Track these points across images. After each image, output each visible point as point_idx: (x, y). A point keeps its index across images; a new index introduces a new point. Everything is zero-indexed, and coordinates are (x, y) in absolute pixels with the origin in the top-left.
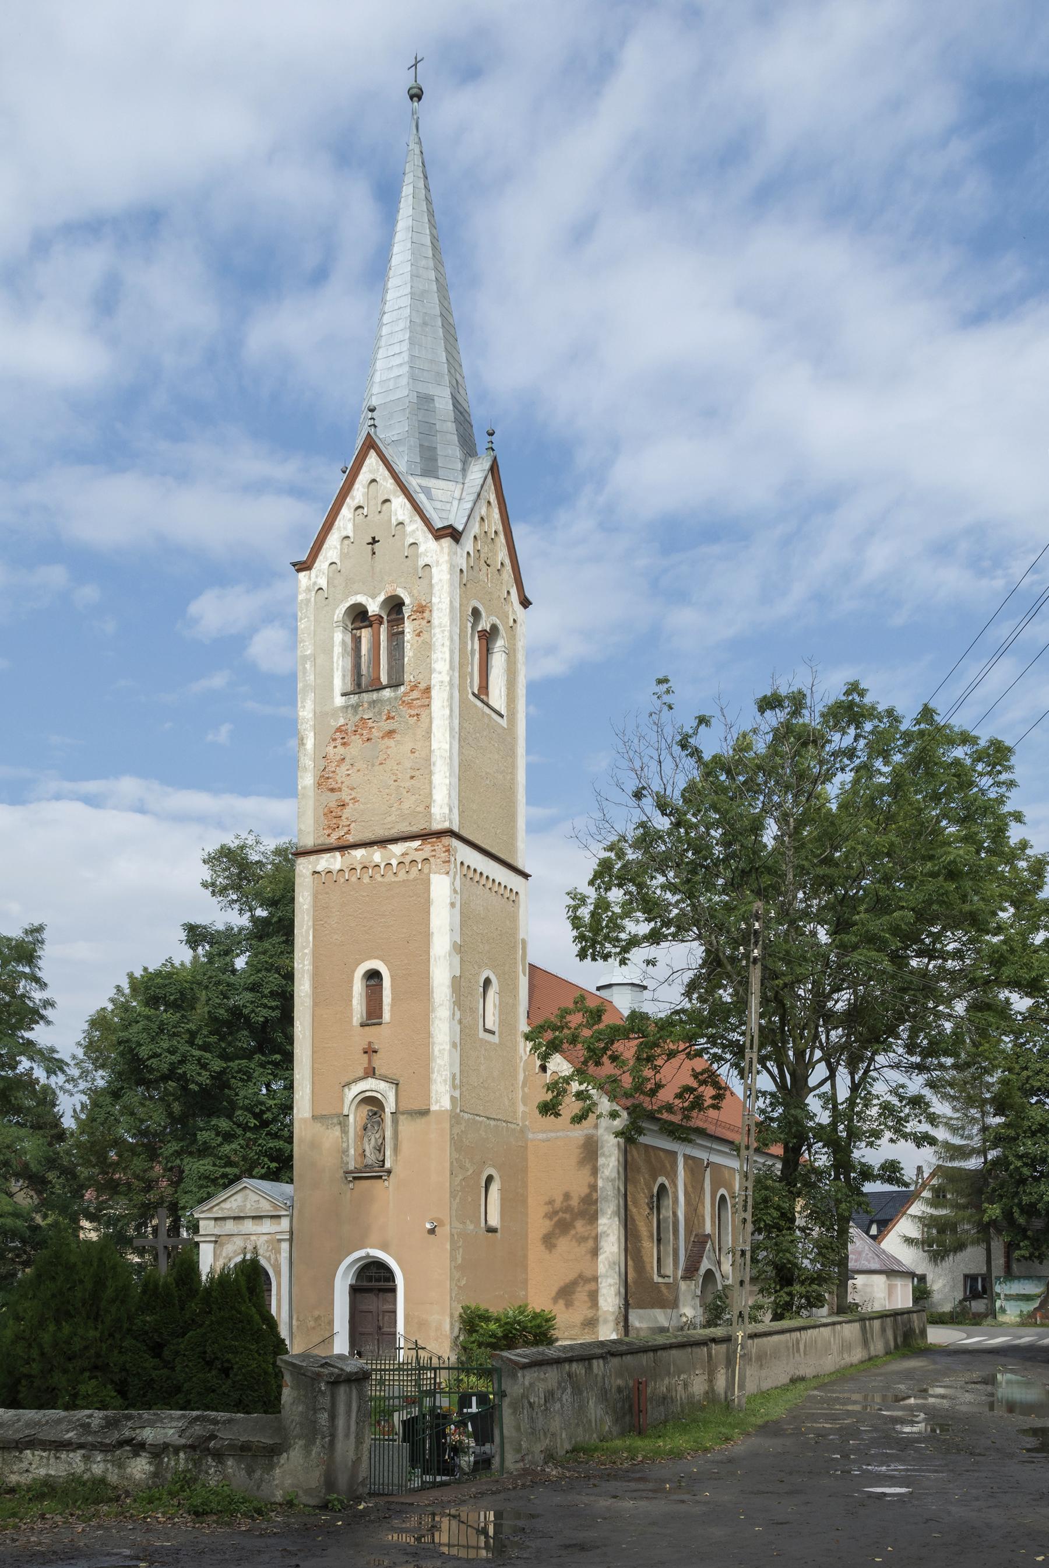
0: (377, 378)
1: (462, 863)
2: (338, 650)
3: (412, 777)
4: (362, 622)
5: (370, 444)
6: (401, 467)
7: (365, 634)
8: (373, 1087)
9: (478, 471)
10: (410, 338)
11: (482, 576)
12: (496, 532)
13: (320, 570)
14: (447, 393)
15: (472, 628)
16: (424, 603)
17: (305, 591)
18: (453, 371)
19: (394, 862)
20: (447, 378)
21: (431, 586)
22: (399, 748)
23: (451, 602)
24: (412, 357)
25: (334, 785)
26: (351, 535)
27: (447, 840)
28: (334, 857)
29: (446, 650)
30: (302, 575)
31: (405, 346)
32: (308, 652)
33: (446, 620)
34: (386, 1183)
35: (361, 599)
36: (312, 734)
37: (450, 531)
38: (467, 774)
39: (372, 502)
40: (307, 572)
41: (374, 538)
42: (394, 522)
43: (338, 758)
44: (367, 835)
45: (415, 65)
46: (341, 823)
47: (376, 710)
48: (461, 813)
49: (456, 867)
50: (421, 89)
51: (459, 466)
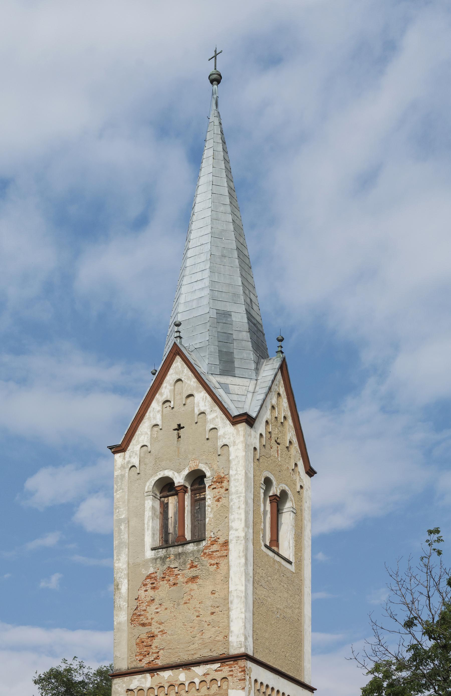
0: (182, 300)
1: (256, 681)
2: (148, 514)
3: (212, 613)
4: (169, 491)
5: (176, 351)
6: (203, 368)
7: (172, 501)
9: (269, 369)
10: (210, 268)
11: (273, 452)
12: (285, 418)
13: (133, 452)
14: (242, 309)
15: (265, 493)
17: (120, 469)
18: (247, 292)
19: (197, 681)
20: (242, 297)
21: (229, 461)
22: (202, 590)
23: (246, 474)
24: (213, 282)
25: (145, 621)
26: (159, 423)
27: (242, 663)
28: (145, 678)
29: (242, 512)
30: (117, 456)
31: (206, 274)
32: (123, 517)
33: (242, 488)
35: (168, 473)
36: (126, 581)
37: (245, 417)
38: (260, 609)
39: (178, 397)
40: (123, 453)
41: (179, 425)
42: (197, 412)
43: (148, 599)
44: (174, 659)
45: (215, 57)
46: (151, 651)
47: (182, 560)
48: (255, 641)
49: (250, 683)
50: (220, 75)
51: (253, 366)
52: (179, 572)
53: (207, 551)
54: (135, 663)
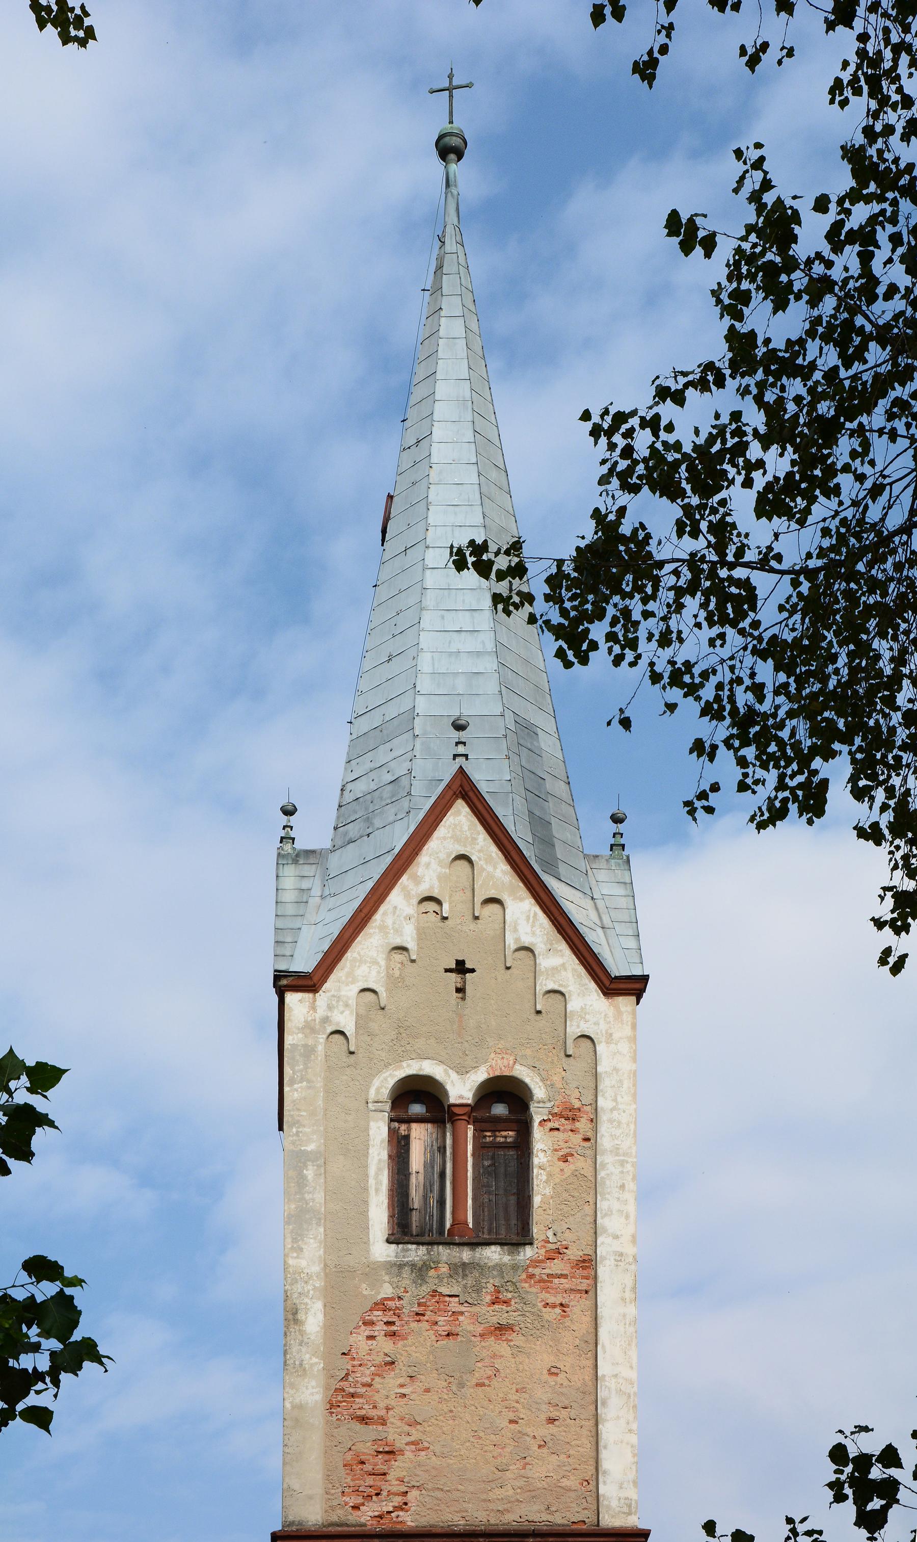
3: (551, 1421)
16: (577, 1104)
25: (367, 1411)
36: (318, 1306)
43: (379, 1359)
44: (449, 1517)
46: (386, 1488)
47: (470, 1281)
52: (462, 1309)
53: (537, 1271)
54: (340, 1512)
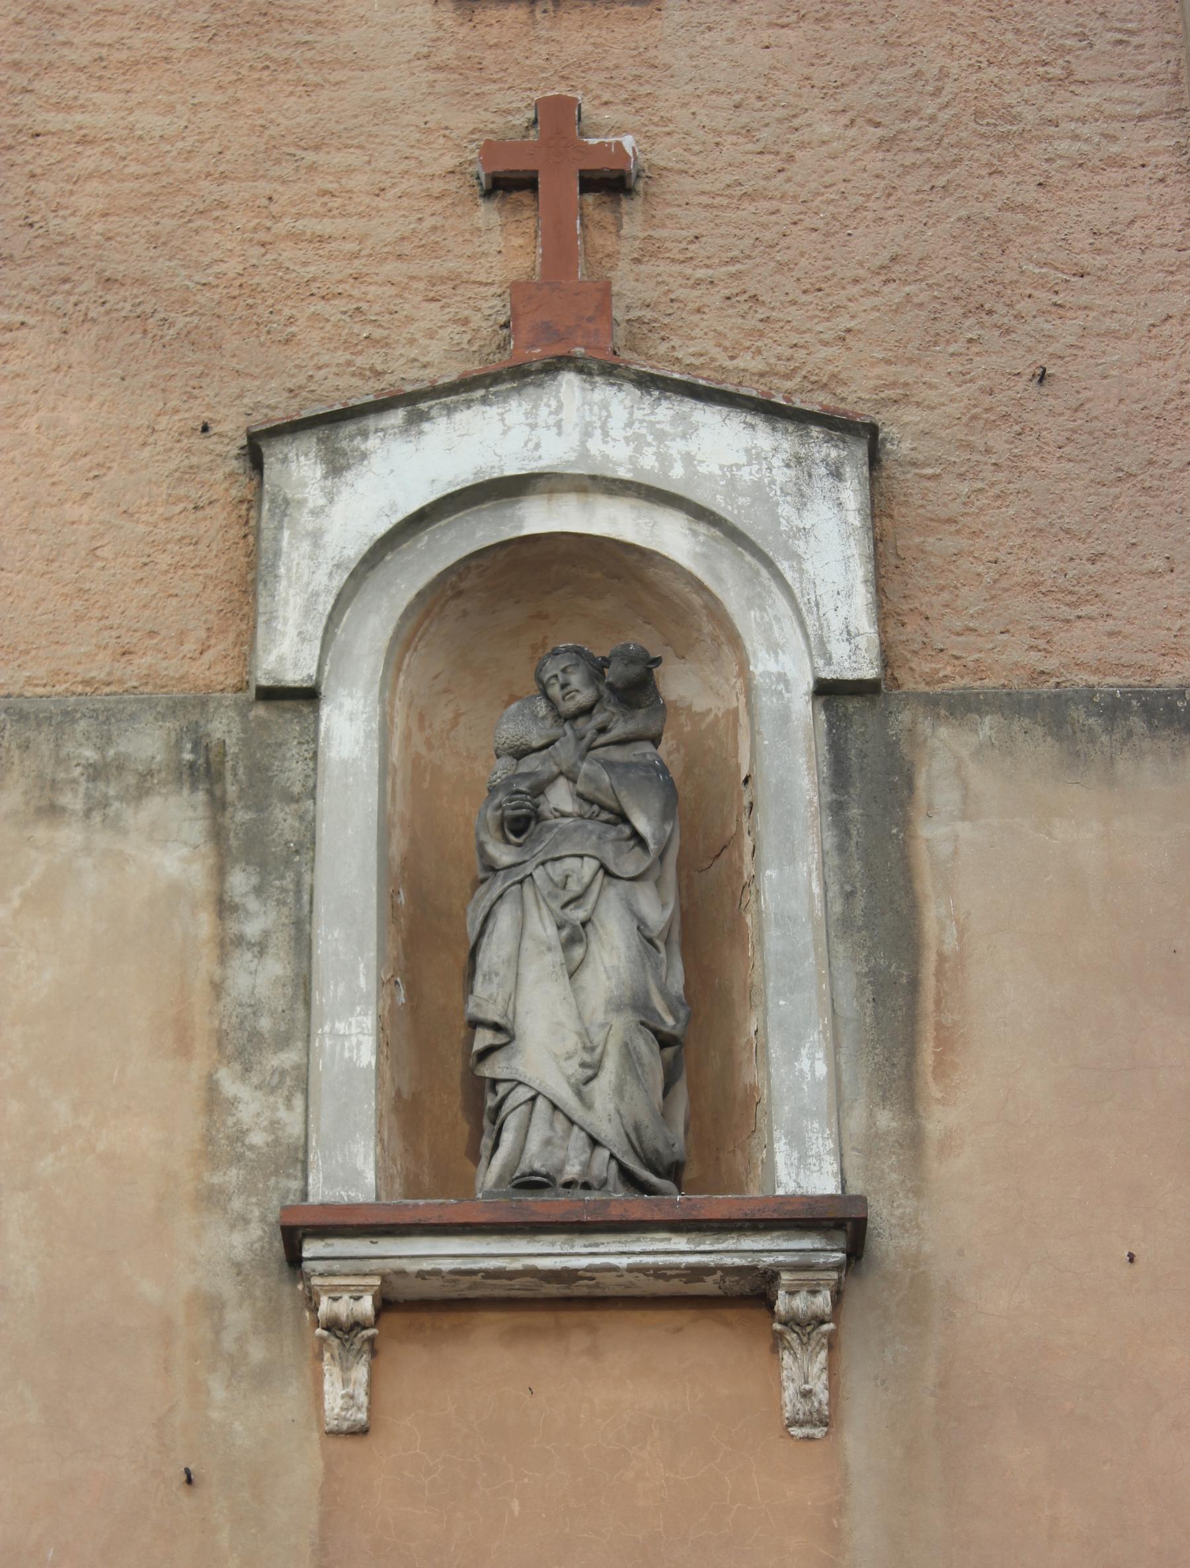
8: (618, 456)
34: (802, 1372)
